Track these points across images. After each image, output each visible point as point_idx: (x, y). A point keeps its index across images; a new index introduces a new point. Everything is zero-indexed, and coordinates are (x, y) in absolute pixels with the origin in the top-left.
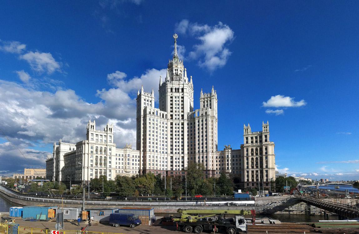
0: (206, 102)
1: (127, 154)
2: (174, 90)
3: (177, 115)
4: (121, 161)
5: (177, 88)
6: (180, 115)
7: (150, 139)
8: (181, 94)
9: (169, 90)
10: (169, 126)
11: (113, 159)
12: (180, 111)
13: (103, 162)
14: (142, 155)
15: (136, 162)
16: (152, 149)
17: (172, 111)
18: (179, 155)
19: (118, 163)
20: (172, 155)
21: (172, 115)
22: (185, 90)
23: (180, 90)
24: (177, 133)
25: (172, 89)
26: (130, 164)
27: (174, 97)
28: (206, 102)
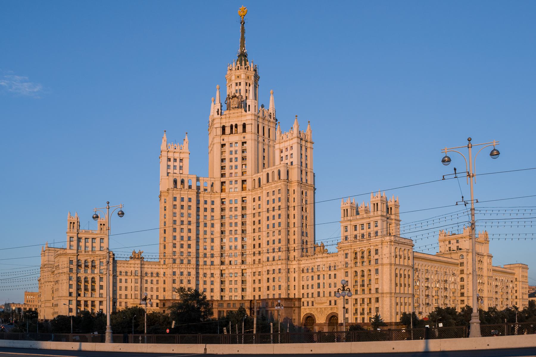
2: (228, 130)
3: (234, 182)
5: (234, 125)
6: (240, 183)
9: (219, 131)
10: (217, 206)
13: (89, 287)
22: (248, 128)
23: (240, 129)
25: (224, 128)
27: (227, 145)
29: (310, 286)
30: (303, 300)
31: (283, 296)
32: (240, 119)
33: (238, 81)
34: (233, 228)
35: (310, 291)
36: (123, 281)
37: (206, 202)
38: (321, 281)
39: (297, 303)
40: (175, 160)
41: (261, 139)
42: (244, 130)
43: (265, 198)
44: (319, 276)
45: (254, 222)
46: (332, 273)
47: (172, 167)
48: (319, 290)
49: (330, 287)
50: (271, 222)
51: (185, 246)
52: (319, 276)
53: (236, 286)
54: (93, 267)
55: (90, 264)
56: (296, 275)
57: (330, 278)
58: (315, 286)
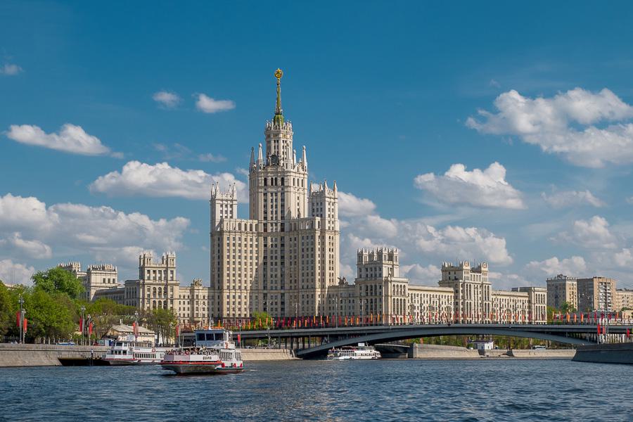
0: (315, 204)
1: (195, 294)
2: (269, 183)
3: (274, 224)
4: (187, 306)
7: (228, 269)
8: (280, 189)
11: (176, 302)
12: (279, 218)
14: (217, 295)
17: (265, 218)
18: (276, 291)
19: (182, 309)
20: (265, 292)
21: (265, 225)
23: (279, 183)
24: (274, 255)
25: (265, 180)
27: (269, 195)
28: (315, 204)
34: (274, 261)
38: (343, 304)
40: (226, 206)
42: (283, 184)
43: (301, 241)
45: (291, 256)
46: (351, 299)
50: (305, 259)
53: (276, 306)
54: (166, 292)
55: (163, 291)
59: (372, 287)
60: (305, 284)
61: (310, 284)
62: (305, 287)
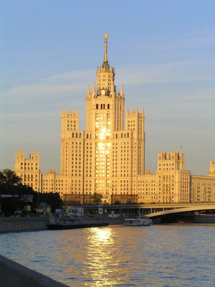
0: (130, 122)
2: (99, 107)
5: (103, 104)
9: (95, 107)
15: (60, 187)
16: (74, 173)
22: (110, 107)
23: (106, 107)
25: (97, 105)
26: (54, 189)
29: (142, 189)
30: (139, 196)
31: (129, 194)
32: (106, 102)
33: (104, 78)
35: (142, 191)
36: (45, 184)
37: (87, 144)
38: (148, 187)
39: (136, 197)
41: (117, 112)
42: (108, 108)
44: (147, 185)
46: (153, 184)
47: (70, 125)
48: (147, 191)
49: (152, 190)
51: (78, 167)
52: (147, 185)
54: (32, 177)
55: (30, 176)
56: (135, 184)
57: (152, 186)
58: (145, 189)
59: (167, 176)
60: (123, 173)
61: (126, 173)
62: (123, 175)
